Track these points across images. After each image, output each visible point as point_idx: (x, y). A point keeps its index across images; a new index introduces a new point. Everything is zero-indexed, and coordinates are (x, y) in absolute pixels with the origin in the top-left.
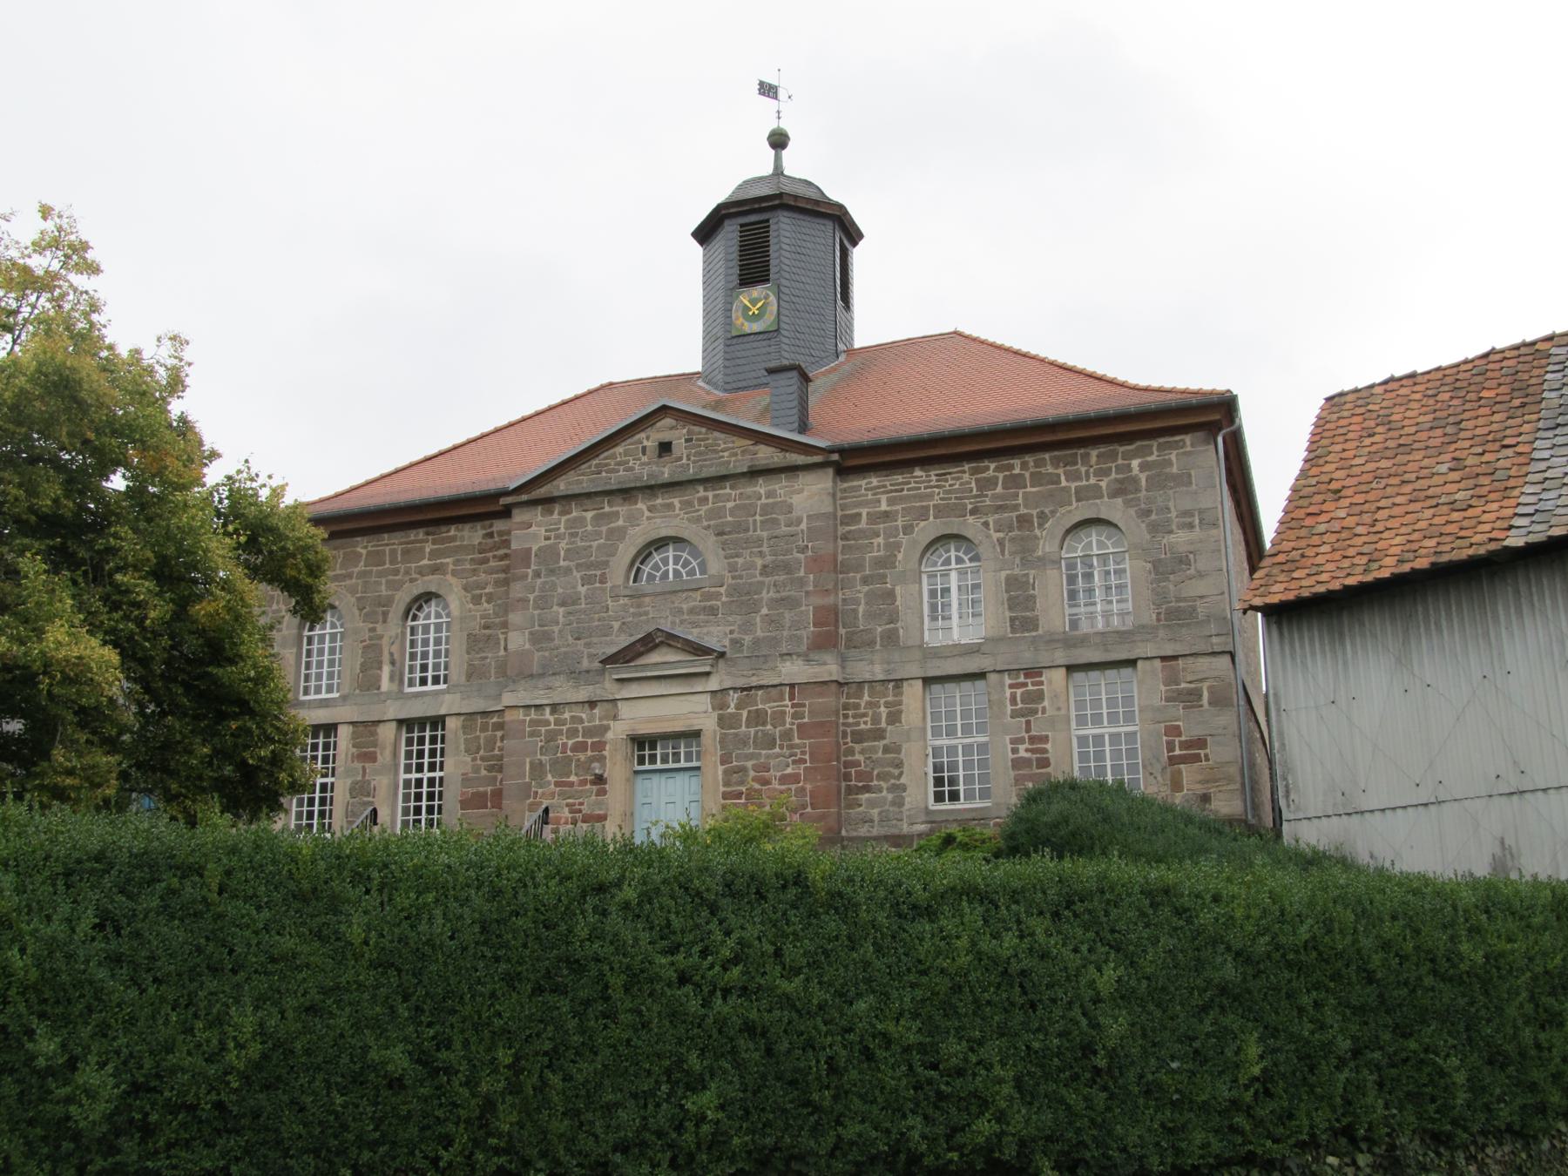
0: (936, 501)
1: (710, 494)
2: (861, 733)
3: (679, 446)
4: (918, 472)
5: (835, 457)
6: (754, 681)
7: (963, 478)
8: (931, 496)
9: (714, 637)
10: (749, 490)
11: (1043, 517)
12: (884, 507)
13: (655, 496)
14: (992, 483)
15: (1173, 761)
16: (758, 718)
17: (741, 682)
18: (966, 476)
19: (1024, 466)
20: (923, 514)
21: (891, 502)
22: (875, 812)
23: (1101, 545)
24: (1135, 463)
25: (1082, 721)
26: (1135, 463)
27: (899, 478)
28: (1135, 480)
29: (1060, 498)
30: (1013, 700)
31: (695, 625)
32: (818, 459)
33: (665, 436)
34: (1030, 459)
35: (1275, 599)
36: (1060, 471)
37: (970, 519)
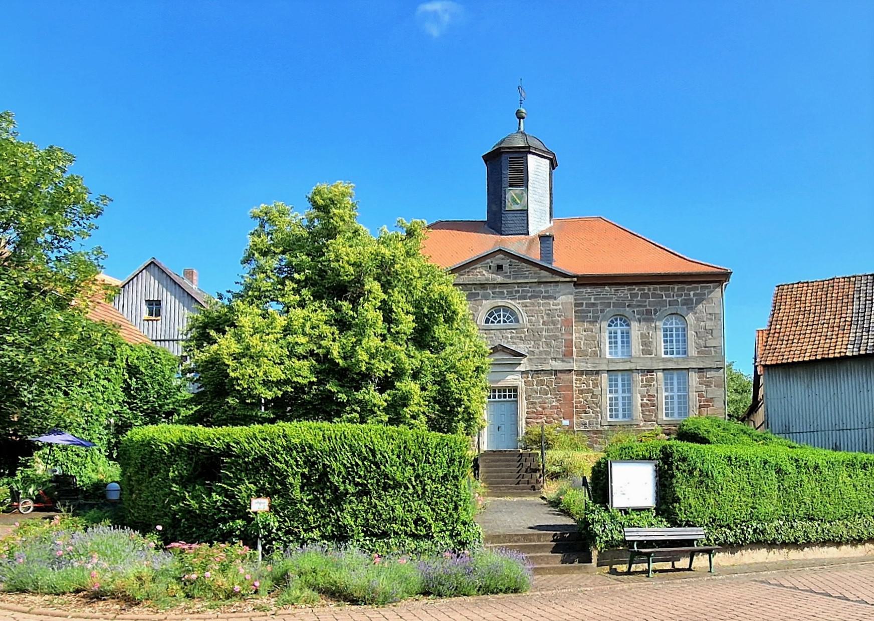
0: (614, 300)
1: (520, 289)
2: (582, 390)
3: (506, 266)
4: (607, 288)
5: (575, 279)
6: (540, 368)
7: (625, 292)
8: (611, 298)
9: (521, 348)
10: (537, 289)
11: (656, 312)
12: (593, 301)
13: (495, 288)
14: (636, 295)
15: (700, 407)
16: (541, 383)
17: (534, 368)
18: (626, 292)
19: (649, 290)
20: (609, 305)
21: (595, 299)
22: (587, 421)
23: (676, 324)
24: (692, 293)
25: (616, 399)
26: (692, 293)
27: (599, 290)
28: (692, 300)
29: (663, 304)
30: (642, 381)
31: (514, 343)
32: (568, 279)
33: (500, 262)
34: (652, 287)
35: (768, 363)
36: (663, 293)
37: (627, 309)
